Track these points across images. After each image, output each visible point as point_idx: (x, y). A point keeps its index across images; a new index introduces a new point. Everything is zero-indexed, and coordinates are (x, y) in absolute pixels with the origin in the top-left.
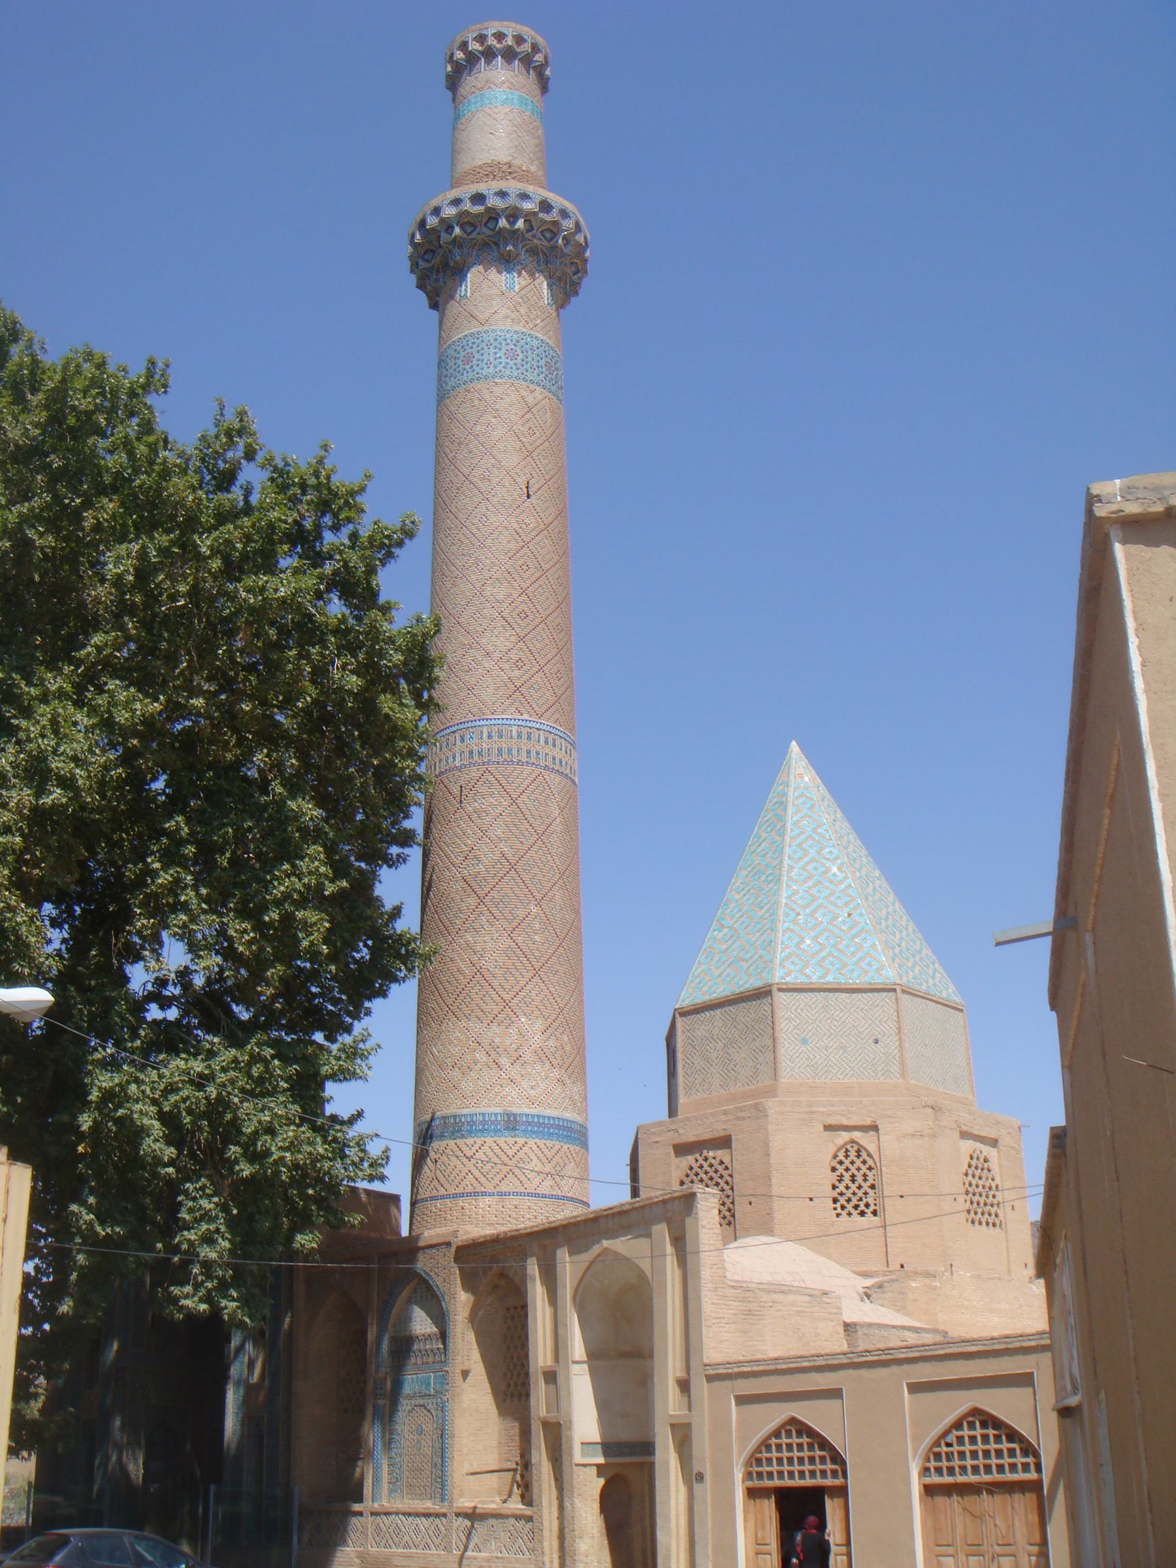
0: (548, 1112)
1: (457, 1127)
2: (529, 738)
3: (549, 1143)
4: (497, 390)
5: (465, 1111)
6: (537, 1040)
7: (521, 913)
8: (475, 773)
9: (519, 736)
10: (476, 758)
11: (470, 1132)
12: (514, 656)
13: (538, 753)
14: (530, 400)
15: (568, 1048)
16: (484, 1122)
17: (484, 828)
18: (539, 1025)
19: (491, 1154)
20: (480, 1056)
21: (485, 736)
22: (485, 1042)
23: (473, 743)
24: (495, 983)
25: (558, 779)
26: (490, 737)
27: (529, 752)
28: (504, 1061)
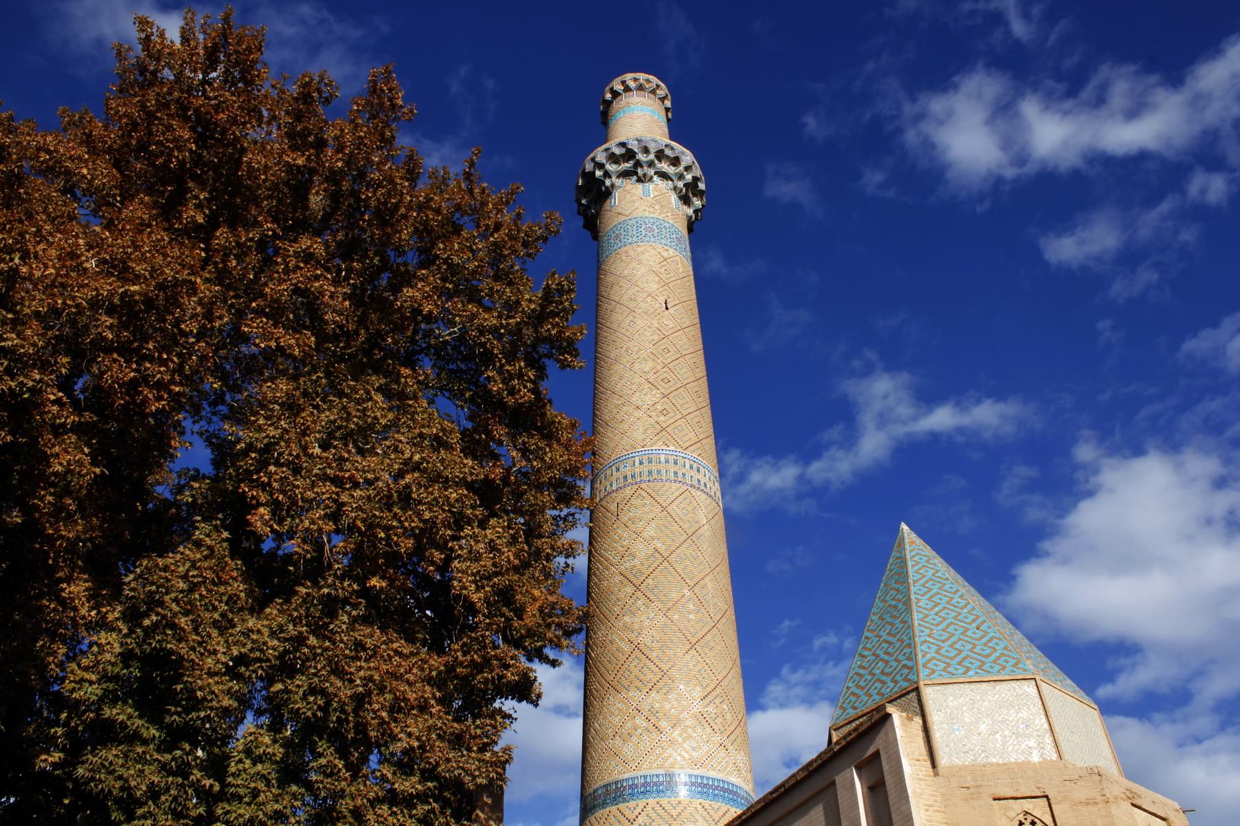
0: (712, 774)
1: (617, 793)
2: (676, 463)
3: (716, 805)
4: (640, 250)
5: (626, 776)
6: (697, 707)
7: (674, 595)
8: (628, 491)
9: (667, 461)
10: (630, 480)
11: (632, 795)
12: (659, 407)
13: (684, 475)
14: (665, 254)
15: (728, 716)
16: (645, 785)
17: (638, 531)
18: (698, 692)
19: (654, 816)
20: (640, 721)
21: (637, 464)
22: (645, 707)
23: (627, 471)
24: (653, 655)
25: (704, 496)
26: (641, 463)
27: (676, 473)
28: (664, 724)
